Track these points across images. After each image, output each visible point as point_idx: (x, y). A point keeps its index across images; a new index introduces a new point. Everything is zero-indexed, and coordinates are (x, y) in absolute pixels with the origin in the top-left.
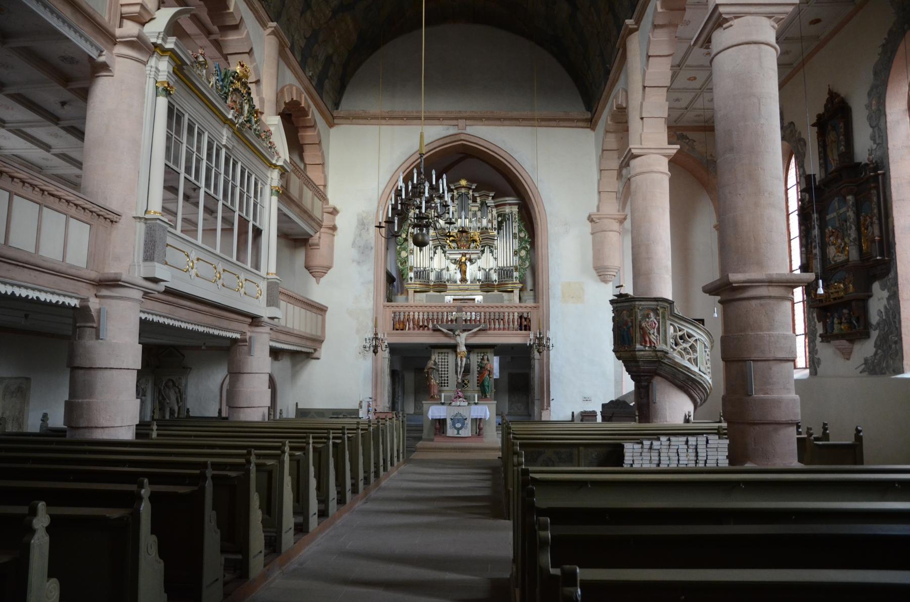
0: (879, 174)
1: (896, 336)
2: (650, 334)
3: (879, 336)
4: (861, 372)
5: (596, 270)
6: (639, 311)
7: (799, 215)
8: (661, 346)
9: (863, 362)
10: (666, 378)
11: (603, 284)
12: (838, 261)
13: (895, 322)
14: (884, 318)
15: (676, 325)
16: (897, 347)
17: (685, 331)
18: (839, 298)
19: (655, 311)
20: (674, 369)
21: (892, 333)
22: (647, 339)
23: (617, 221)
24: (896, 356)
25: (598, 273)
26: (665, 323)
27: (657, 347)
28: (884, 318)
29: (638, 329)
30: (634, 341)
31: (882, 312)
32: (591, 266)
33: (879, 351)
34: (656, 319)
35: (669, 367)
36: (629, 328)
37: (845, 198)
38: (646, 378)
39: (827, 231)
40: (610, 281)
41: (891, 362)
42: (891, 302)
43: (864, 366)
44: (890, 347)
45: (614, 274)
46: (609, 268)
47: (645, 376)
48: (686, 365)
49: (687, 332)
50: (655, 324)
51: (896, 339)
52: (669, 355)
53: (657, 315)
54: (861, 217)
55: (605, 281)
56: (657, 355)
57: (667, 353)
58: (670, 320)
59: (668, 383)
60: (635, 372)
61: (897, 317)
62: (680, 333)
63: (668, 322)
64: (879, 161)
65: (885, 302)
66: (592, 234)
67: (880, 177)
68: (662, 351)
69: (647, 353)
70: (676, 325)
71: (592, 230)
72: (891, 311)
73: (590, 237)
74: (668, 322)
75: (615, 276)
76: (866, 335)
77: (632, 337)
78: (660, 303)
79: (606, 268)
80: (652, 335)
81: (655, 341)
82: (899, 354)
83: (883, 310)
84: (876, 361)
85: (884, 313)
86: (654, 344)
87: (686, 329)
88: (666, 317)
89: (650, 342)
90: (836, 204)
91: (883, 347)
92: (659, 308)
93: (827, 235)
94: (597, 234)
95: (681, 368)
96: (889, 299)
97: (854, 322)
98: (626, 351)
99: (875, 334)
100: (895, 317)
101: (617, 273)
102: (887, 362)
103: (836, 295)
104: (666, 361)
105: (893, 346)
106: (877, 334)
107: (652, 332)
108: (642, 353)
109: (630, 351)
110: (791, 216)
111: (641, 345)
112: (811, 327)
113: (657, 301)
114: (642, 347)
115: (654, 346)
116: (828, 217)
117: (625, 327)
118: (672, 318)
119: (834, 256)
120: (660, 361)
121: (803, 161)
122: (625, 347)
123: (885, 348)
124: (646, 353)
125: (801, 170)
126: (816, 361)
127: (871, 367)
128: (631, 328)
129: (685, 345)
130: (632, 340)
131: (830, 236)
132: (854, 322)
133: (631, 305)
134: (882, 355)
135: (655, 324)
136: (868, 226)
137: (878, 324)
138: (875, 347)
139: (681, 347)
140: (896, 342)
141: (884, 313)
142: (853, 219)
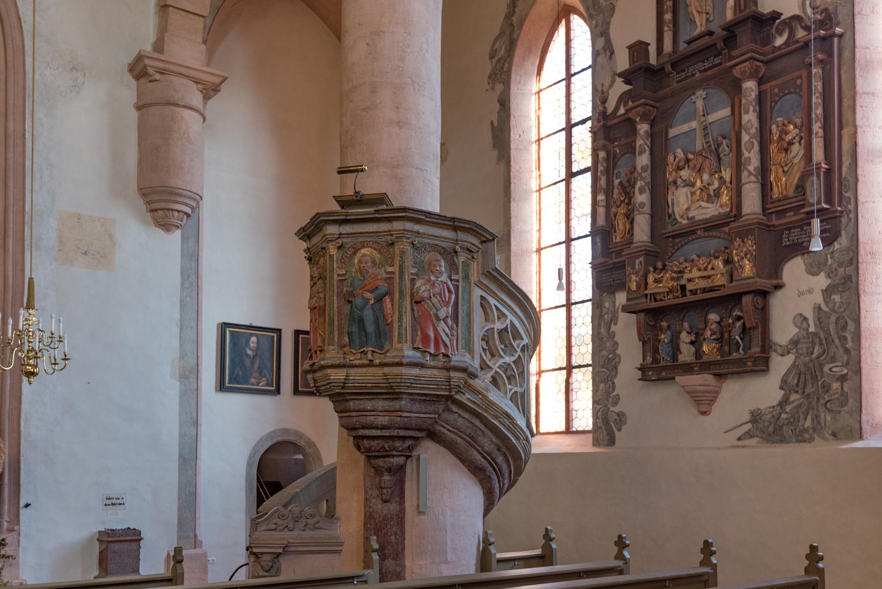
0: (834, 35)
1: (846, 365)
2: (438, 318)
3: (794, 366)
4: (739, 439)
5: (144, 195)
6: (409, 250)
7: (594, 132)
8: (460, 358)
9: (747, 417)
10: (450, 446)
11: (159, 232)
12: (697, 218)
13: (843, 339)
14: (812, 329)
15: (492, 301)
16: (846, 389)
17: (508, 322)
18: (711, 290)
19: (450, 255)
20: (477, 423)
21: (833, 359)
22: (432, 334)
23: (201, 87)
24: (842, 406)
25: (148, 203)
26: (470, 293)
27: (454, 358)
28: (812, 329)
29: (407, 303)
30: (396, 338)
31: (805, 319)
32: (133, 184)
33: (794, 397)
34: (451, 280)
35: (466, 415)
36: (380, 300)
37: (740, 88)
38: (409, 443)
39: (671, 158)
40: (177, 227)
41: (828, 418)
42: (836, 298)
43: (749, 426)
44: (827, 388)
45: (188, 210)
46: (171, 193)
47: (404, 438)
48: (509, 411)
49: (511, 322)
50: (450, 291)
51: (845, 371)
52: (477, 383)
53: (453, 267)
54: (774, 127)
55: (166, 226)
56: (449, 379)
57: (473, 376)
58: (480, 285)
59: (451, 458)
60: (384, 428)
61: (851, 327)
62: (498, 326)
63: (477, 292)
64: (830, 8)
65: (819, 298)
66: (139, 108)
67: (836, 40)
68: (464, 370)
69: (429, 372)
70: (492, 301)
71: (139, 96)
72: (833, 318)
73: (134, 114)
74: (477, 292)
75: (188, 215)
76: (761, 365)
77: (390, 325)
78: (461, 236)
79: (173, 193)
80: (442, 322)
81: (447, 341)
82: (851, 401)
83: (810, 315)
84: (784, 416)
85: (811, 322)
86: (446, 345)
87: (510, 317)
88: (474, 278)
89: (437, 340)
90: (700, 104)
91: (804, 388)
92: (457, 248)
93: (670, 168)
94: (153, 110)
95: (496, 417)
96: (827, 292)
97: (737, 338)
98: (371, 364)
99: (781, 365)
100: (844, 328)
101: (193, 208)
102: (816, 417)
103: (704, 284)
104: (465, 398)
105: (836, 386)
106: (792, 362)
107: (442, 313)
108: (415, 371)
109: (382, 365)
110: (575, 131)
111: (416, 349)
112: (604, 353)
113: (455, 229)
114: (418, 354)
115: (446, 355)
116: (673, 132)
117: (368, 295)
118: (486, 282)
119: (688, 209)
120: (449, 398)
121: (609, 23)
122: (366, 353)
123: (809, 389)
124: (424, 372)
125: (601, 41)
126: (612, 417)
127: (771, 429)
128: (387, 299)
129: (508, 359)
130: (391, 331)
131: (679, 169)
132: (737, 338)
133: (389, 233)
134: (800, 406)
135: (450, 291)
136: (790, 143)
137: (795, 343)
138: (781, 388)
139: (501, 361)
140: (843, 378)
141: (811, 322)
142: (756, 128)
